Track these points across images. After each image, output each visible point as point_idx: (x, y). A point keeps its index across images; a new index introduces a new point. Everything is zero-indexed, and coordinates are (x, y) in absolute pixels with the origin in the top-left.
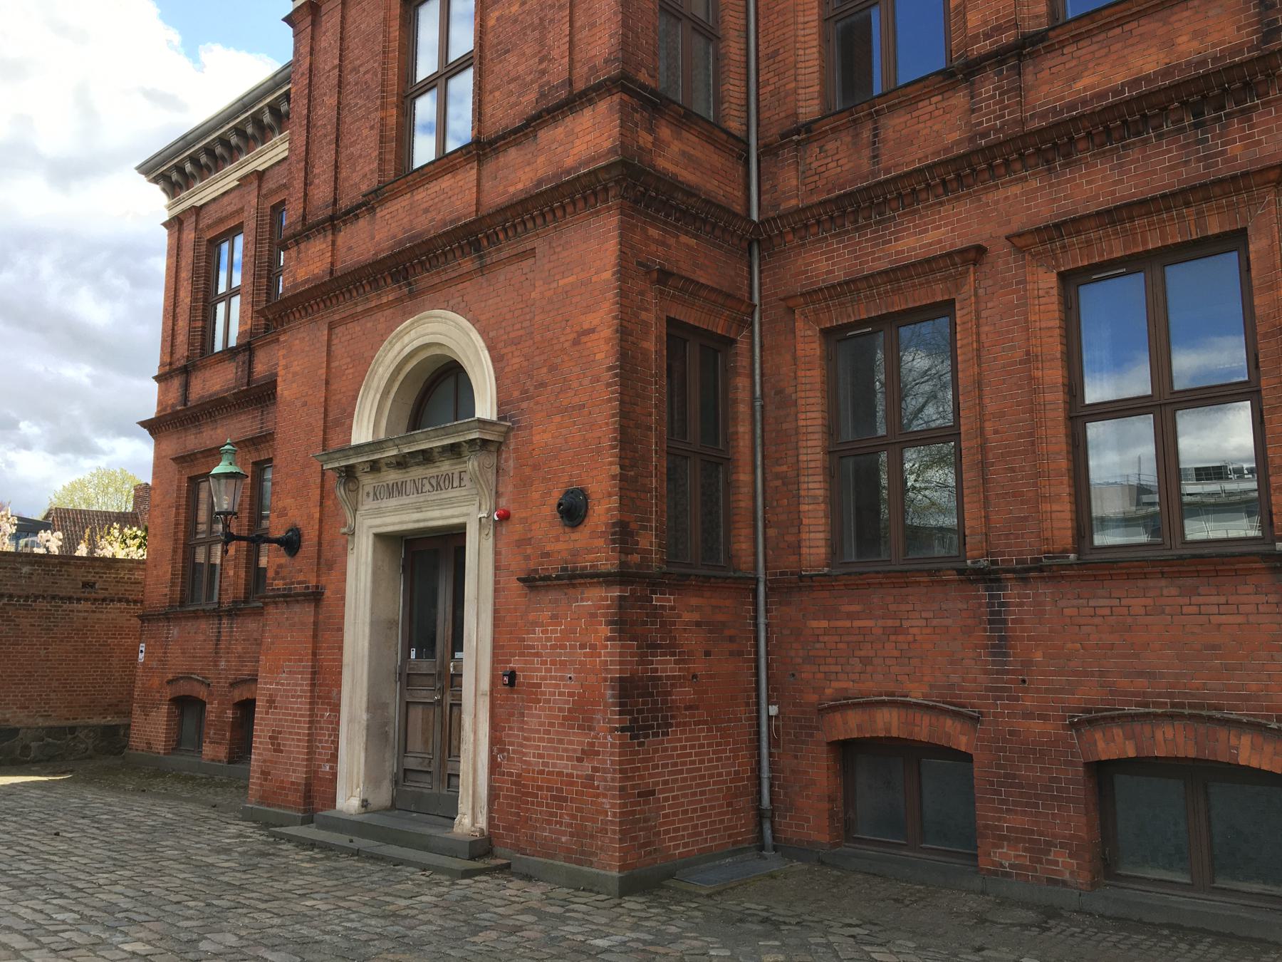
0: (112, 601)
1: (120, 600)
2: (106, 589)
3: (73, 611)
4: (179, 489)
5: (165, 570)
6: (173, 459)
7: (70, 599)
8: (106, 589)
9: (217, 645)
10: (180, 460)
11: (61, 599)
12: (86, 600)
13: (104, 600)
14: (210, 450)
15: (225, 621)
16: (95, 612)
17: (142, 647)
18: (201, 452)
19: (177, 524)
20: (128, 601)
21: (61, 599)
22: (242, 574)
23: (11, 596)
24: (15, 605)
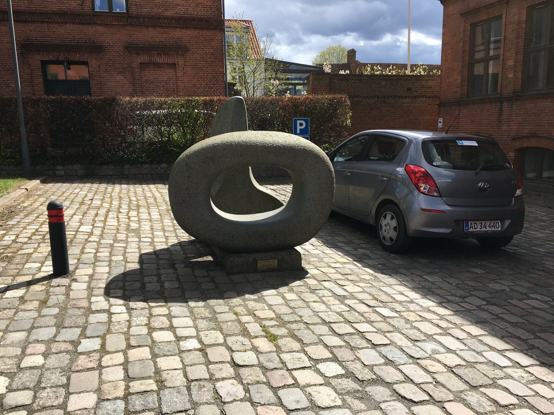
0: (419, 97)
1: (423, 97)
2: (417, 91)
3: (403, 103)
4: (465, 31)
5: (457, 78)
6: (461, 14)
7: (402, 97)
8: (417, 91)
9: (499, 117)
10: (464, 15)
11: (398, 97)
12: (409, 97)
13: (416, 97)
14: (490, 4)
15: (505, 105)
16: (412, 103)
17: (441, 120)
18: (485, 6)
19: (464, 52)
20: (426, 97)
21: (398, 97)
22: (520, 75)
23: (378, 97)
24: (380, 101)
